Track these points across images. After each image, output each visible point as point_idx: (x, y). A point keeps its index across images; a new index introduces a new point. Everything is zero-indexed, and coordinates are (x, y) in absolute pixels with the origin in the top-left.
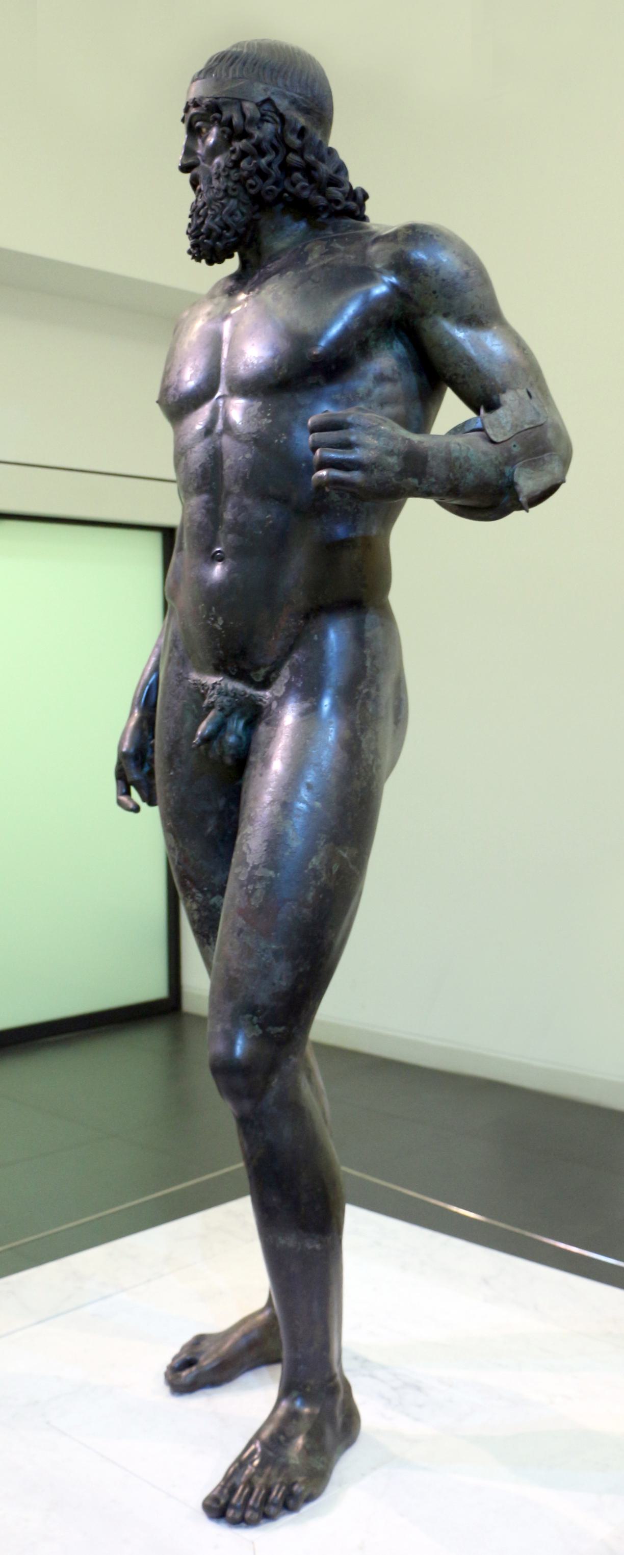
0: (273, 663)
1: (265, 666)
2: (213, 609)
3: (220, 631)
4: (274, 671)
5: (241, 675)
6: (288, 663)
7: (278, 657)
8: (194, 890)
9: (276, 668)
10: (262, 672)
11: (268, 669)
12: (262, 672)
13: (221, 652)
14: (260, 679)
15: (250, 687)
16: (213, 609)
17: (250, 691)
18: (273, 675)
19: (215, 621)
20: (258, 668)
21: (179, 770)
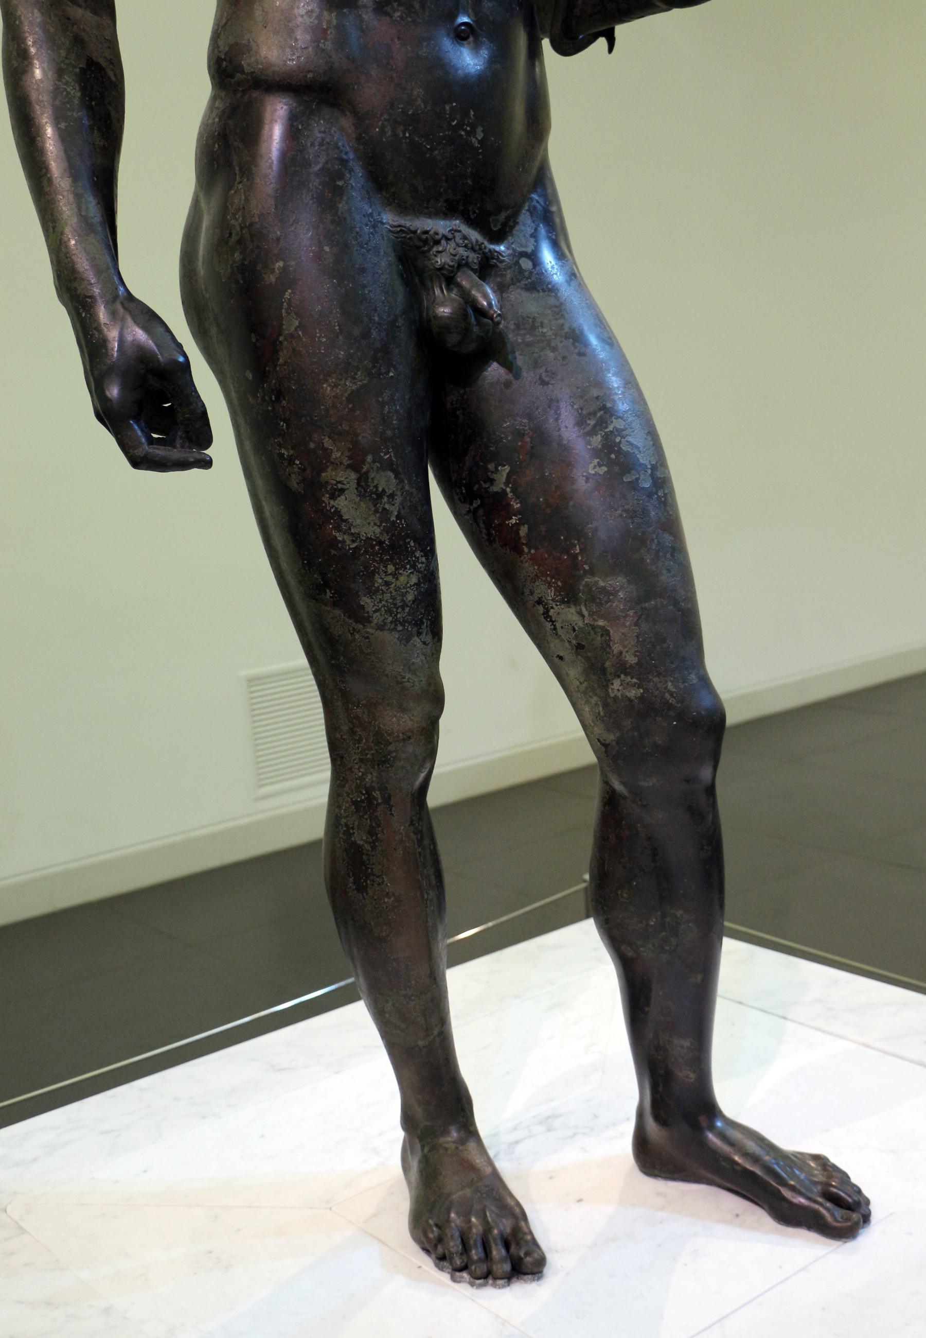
2: (472, 113)
3: (477, 149)
8: (418, 554)
13: (469, 182)
16: (472, 113)
19: (473, 132)
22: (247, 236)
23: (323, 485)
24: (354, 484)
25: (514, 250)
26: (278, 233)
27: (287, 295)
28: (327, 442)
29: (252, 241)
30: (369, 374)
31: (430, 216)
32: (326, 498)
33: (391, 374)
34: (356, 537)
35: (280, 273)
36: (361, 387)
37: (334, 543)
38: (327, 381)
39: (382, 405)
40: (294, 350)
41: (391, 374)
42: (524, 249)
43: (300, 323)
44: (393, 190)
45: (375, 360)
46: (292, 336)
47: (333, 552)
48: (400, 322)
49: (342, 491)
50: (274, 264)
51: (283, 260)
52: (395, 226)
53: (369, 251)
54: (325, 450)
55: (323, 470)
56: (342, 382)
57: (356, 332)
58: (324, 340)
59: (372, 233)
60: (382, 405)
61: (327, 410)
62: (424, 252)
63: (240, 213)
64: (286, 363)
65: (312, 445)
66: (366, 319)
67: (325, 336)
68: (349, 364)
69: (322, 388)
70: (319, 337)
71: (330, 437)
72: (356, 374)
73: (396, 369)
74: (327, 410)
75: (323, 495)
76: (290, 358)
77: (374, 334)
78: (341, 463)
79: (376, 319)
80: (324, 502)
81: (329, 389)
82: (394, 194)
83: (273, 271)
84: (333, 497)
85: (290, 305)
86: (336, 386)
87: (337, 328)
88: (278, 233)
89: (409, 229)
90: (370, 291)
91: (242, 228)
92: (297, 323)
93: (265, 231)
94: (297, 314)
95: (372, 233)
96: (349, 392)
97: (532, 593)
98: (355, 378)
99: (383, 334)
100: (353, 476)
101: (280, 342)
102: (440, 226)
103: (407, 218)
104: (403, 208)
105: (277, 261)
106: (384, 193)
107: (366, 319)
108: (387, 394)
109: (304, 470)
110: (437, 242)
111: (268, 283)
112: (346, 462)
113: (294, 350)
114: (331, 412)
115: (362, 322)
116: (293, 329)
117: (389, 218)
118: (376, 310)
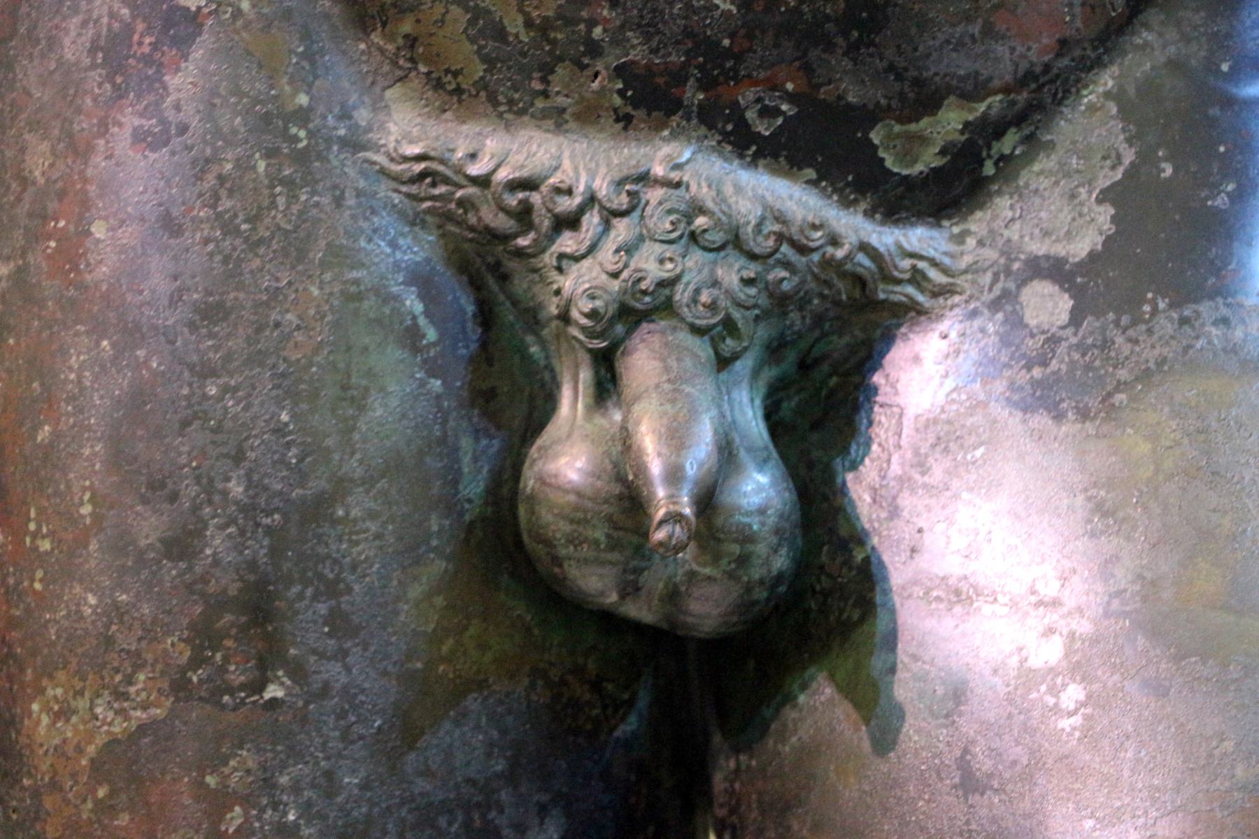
0: (1026, 79)
1: (973, 90)
4: (1019, 120)
5: (826, 146)
6: (1107, 80)
7: (1064, 45)
9: (1037, 99)
10: (950, 121)
11: (993, 104)
12: (950, 121)
14: (928, 160)
15: (846, 204)
17: (855, 228)
18: (1009, 143)
20: (927, 101)
21: (333, 671)
25: (1008, 252)
30: (180, 687)
31: (557, 119)
33: (273, 691)
36: (142, 729)
38: (42, 691)
39: (219, 802)
41: (273, 691)
42: (1060, 250)
44: (407, 27)
45: (204, 637)
48: (357, 505)
52: (406, 159)
53: (254, 245)
56: (82, 704)
57: (149, 527)
58: (46, 545)
59: (289, 183)
60: (219, 802)
62: (520, 253)
66: (189, 490)
67: (51, 534)
68: (109, 641)
69: (30, 713)
70: (35, 536)
72: (129, 681)
73: (298, 672)
74: (36, 794)
77: (217, 543)
79: (237, 489)
81: (45, 720)
82: (412, 41)
86: (64, 713)
87: (86, 510)
89: (459, 170)
90: (225, 389)
95: (289, 183)
96: (100, 740)
98: (125, 696)
99: (259, 548)
102: (573, 161)
103: (469, 128)
104: (450, 92)
106: (376, 38)
107: (189, 490)
108: (241, 766)
110: (570, 222)
114: (48, 803)
115: (174, 497)
117: (406, 129)
118: (238, 458)
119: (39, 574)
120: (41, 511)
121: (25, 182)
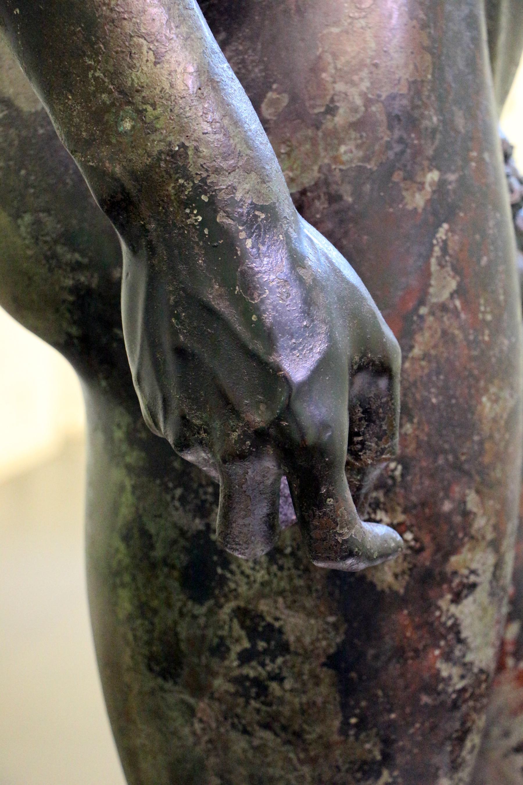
22: (382, 118)
23: (445, 579)
24: (488, 575)
26: (435, 119)
27: (442, 233)
28: (472, 501)
29: (391, 128)
32: (445, 602)
34: (467, 666)
35: (434, 192)
37: (433, 684)
40: (445, 333)
43: (459, 285)
46: (444, 307)
47: (425, 699)
49: (473, 586)
50: (424, 176)
51: (439, 169)
54: (466, 514)
55: (455, 550)
61: (481, 443)
63: (365, 73)
64: (426, 356)
65: (447, 506)
67: (491, 312)
71: (478, 492)
74: (481, 443)
75: (442, 596)
76: (435, 346)
78: (483, 538)
80: (439, 608)
83: (421, 186)
84: (457, 599)
85: (444, 250)
88: (435, 119)
91: (368, 102)
92: (453, 285)
93: (416, 114)
94: (455, 269)
97: (506, 734)
100: (491, 559)
101: (421, 318)
105: (430, 170)
109: (418, 551)
111: (410, 207)
112: (490, 536)
113: (445, 333)
116: (445, 295)
119: (487, 332)
120: (486, 300)
121: (457, 132)
